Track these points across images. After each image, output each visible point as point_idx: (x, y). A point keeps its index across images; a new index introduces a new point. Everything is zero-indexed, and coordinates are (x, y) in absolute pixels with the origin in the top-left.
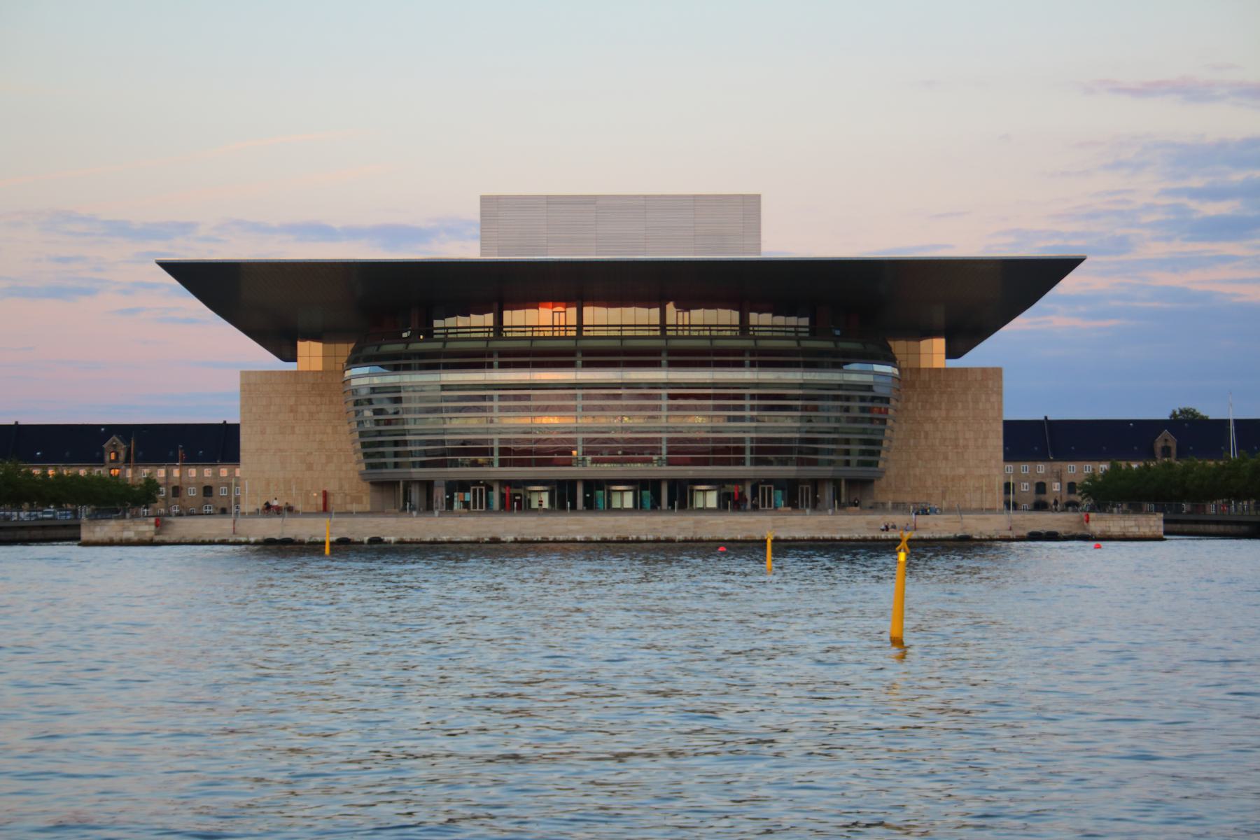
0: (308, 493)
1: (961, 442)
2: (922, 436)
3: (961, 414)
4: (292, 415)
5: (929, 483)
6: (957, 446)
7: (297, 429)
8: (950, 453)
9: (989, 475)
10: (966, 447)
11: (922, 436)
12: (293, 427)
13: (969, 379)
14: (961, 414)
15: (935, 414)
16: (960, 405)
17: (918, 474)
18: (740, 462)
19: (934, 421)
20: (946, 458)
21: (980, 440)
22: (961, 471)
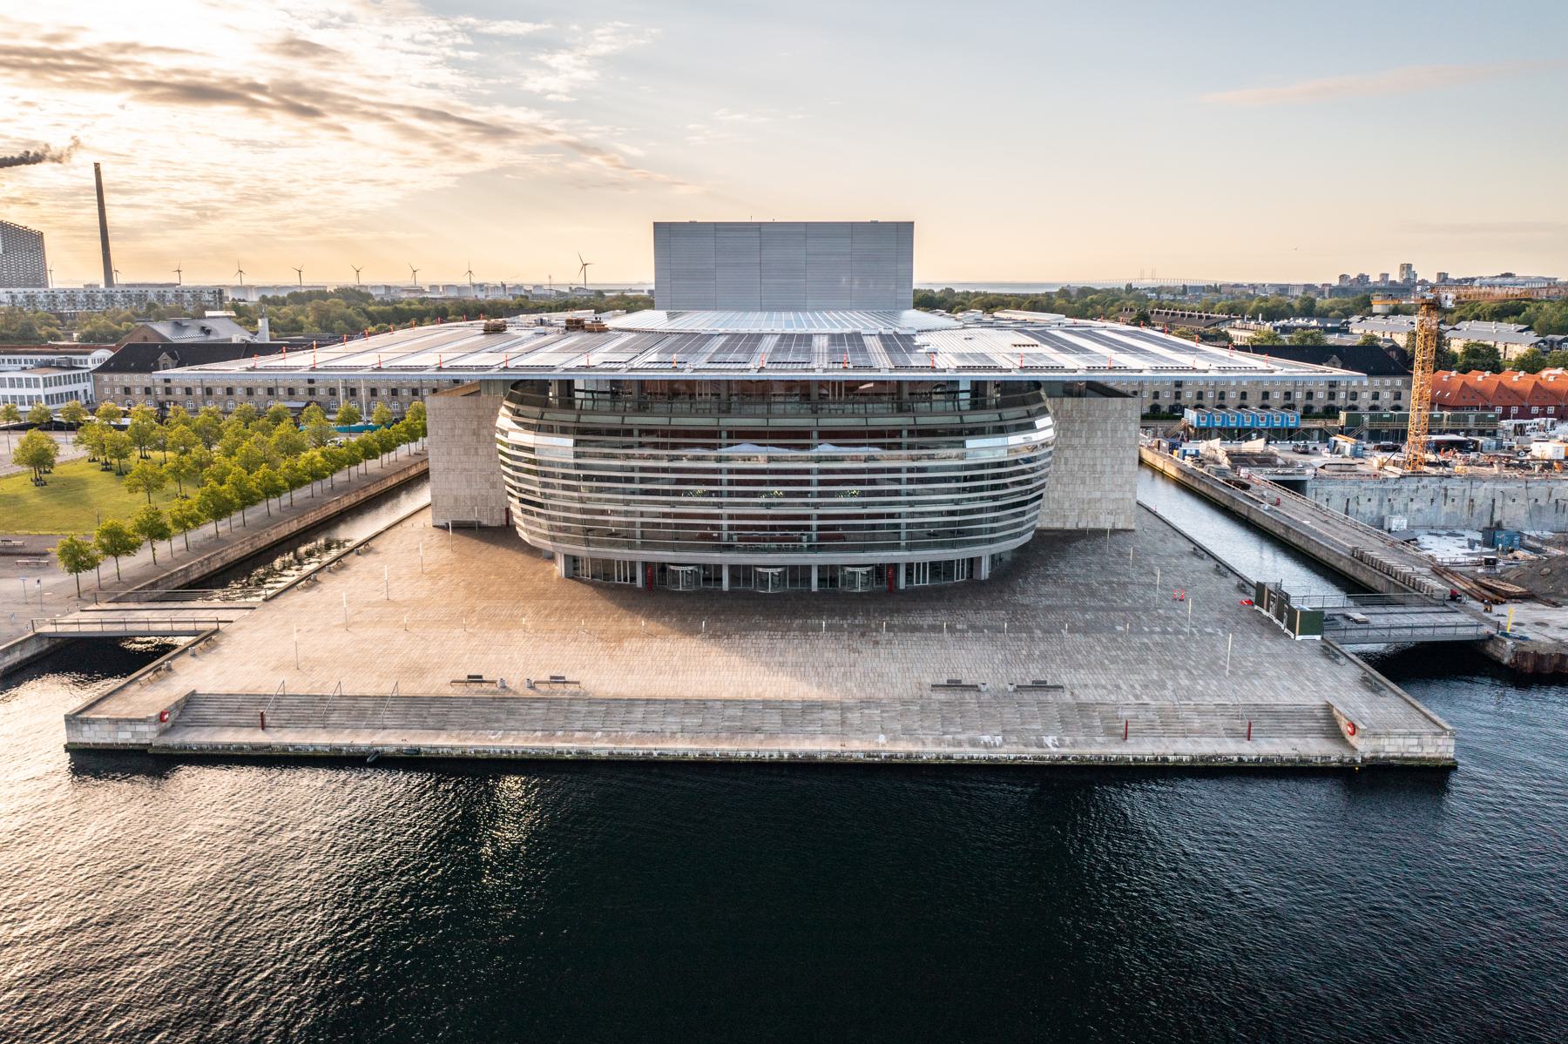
0: (492, 509)
1: (1099, 468)
2: (1063, 460)
3: (1100, 441)
4: (475, 437)
5: (1067, 505)
6: (1094, 472)
7: (480, 451)
8: (1088, 479)
9: (1123, 499)
10: (1103, 473)
11: (1063, 460)
12: (476, 449)
13: (1110, 408)
14: (1100, 441)
15: (1075, 441)
16: (1099, 433)
17: (1056, 496)
18: (896, 547)
19: (1074, 448)
20: (1084, 483)
21: (1116, 467)
22: (1098, 495)
